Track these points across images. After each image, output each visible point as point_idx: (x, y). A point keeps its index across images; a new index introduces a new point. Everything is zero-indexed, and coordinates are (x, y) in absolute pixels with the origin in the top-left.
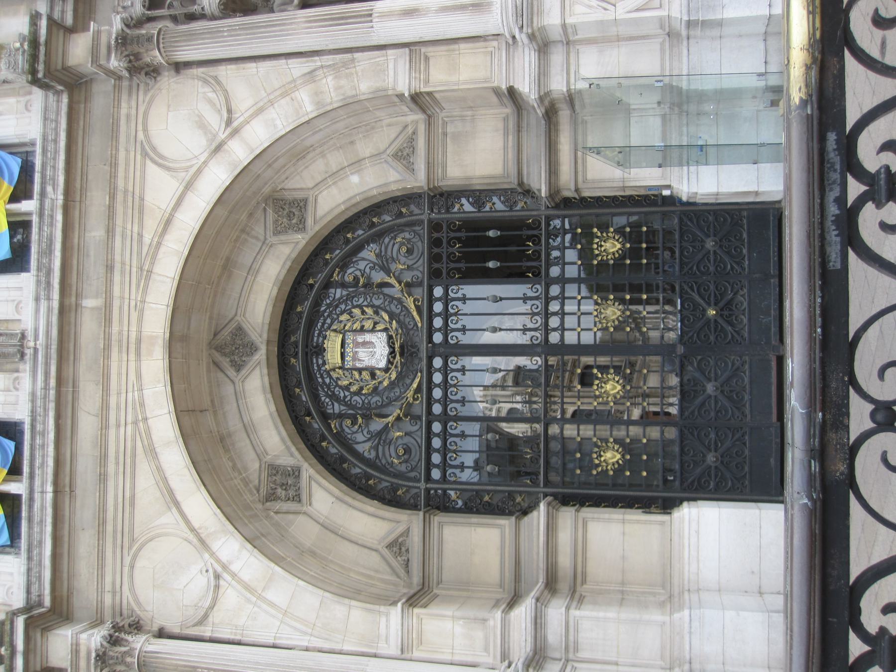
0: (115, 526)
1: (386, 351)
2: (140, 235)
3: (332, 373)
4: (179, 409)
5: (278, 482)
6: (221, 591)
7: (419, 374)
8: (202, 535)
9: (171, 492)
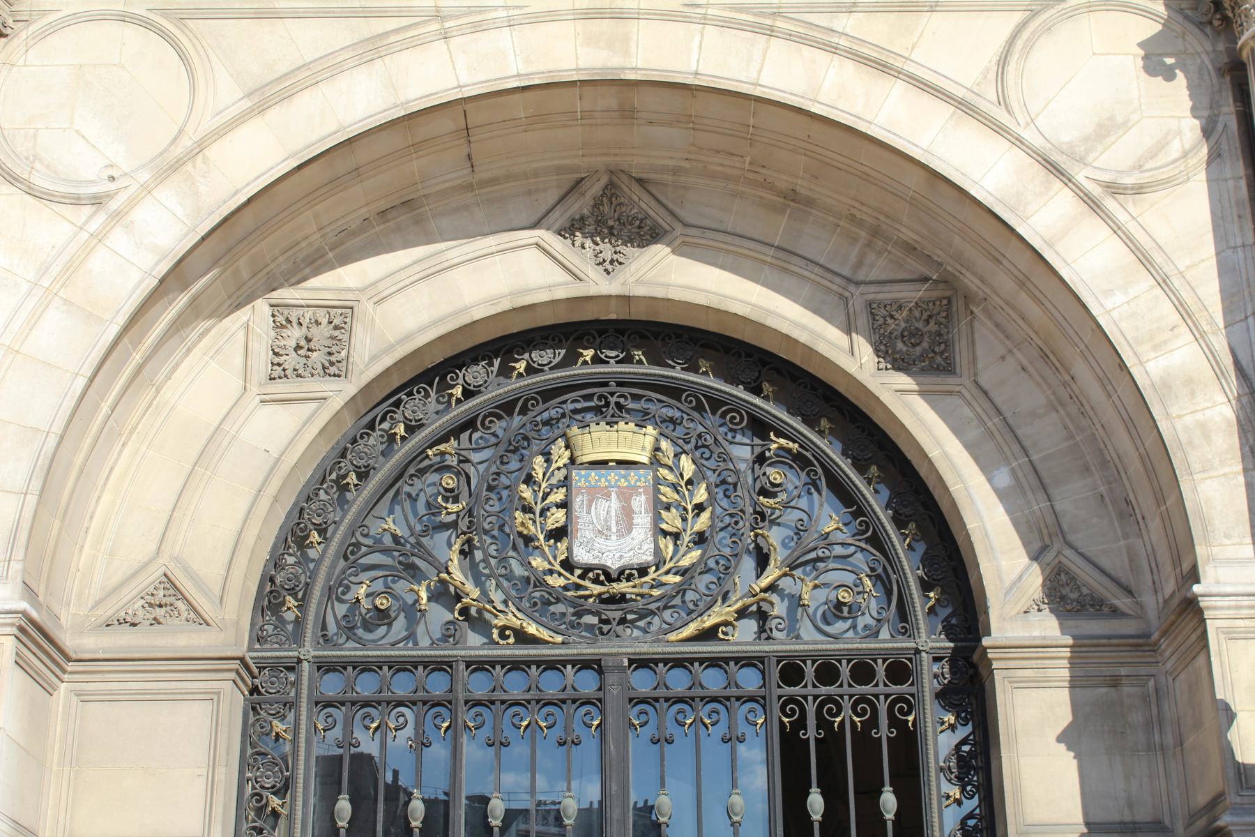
1: (613, 564)
3: (561, 442)
4: (468, 107)
5: (315, 332)
6: (67, 211)
7: (559, 639)
8: (190, 164)
9: (287, 96)
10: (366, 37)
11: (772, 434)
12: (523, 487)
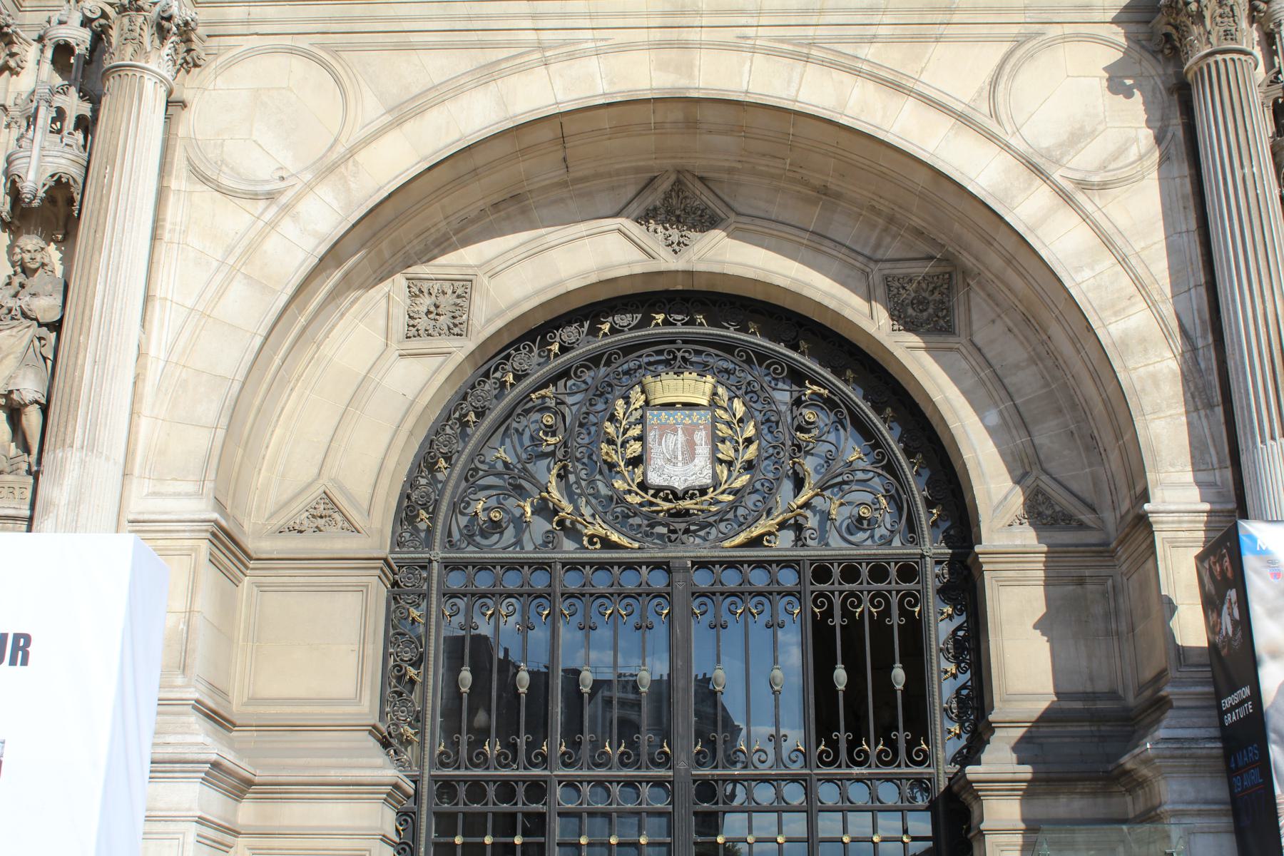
0: (361, 19)
1: (679, 485)
2: (872, 40)
4: (564, 120)
5: (442, 300)
6: (247, 204)
7: (636, 545)
8: (343, 166)
9: (420, 111)
10: (483, 64)
11: (807, 382)
12: (607, 424)
